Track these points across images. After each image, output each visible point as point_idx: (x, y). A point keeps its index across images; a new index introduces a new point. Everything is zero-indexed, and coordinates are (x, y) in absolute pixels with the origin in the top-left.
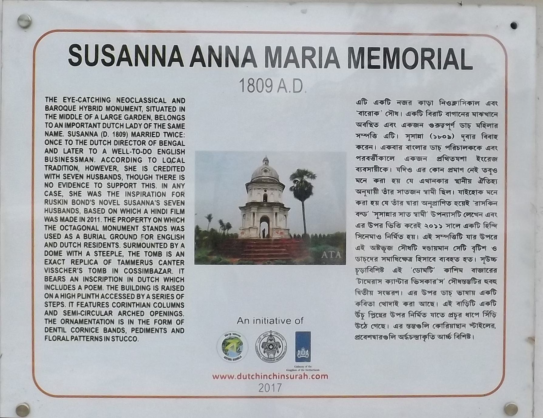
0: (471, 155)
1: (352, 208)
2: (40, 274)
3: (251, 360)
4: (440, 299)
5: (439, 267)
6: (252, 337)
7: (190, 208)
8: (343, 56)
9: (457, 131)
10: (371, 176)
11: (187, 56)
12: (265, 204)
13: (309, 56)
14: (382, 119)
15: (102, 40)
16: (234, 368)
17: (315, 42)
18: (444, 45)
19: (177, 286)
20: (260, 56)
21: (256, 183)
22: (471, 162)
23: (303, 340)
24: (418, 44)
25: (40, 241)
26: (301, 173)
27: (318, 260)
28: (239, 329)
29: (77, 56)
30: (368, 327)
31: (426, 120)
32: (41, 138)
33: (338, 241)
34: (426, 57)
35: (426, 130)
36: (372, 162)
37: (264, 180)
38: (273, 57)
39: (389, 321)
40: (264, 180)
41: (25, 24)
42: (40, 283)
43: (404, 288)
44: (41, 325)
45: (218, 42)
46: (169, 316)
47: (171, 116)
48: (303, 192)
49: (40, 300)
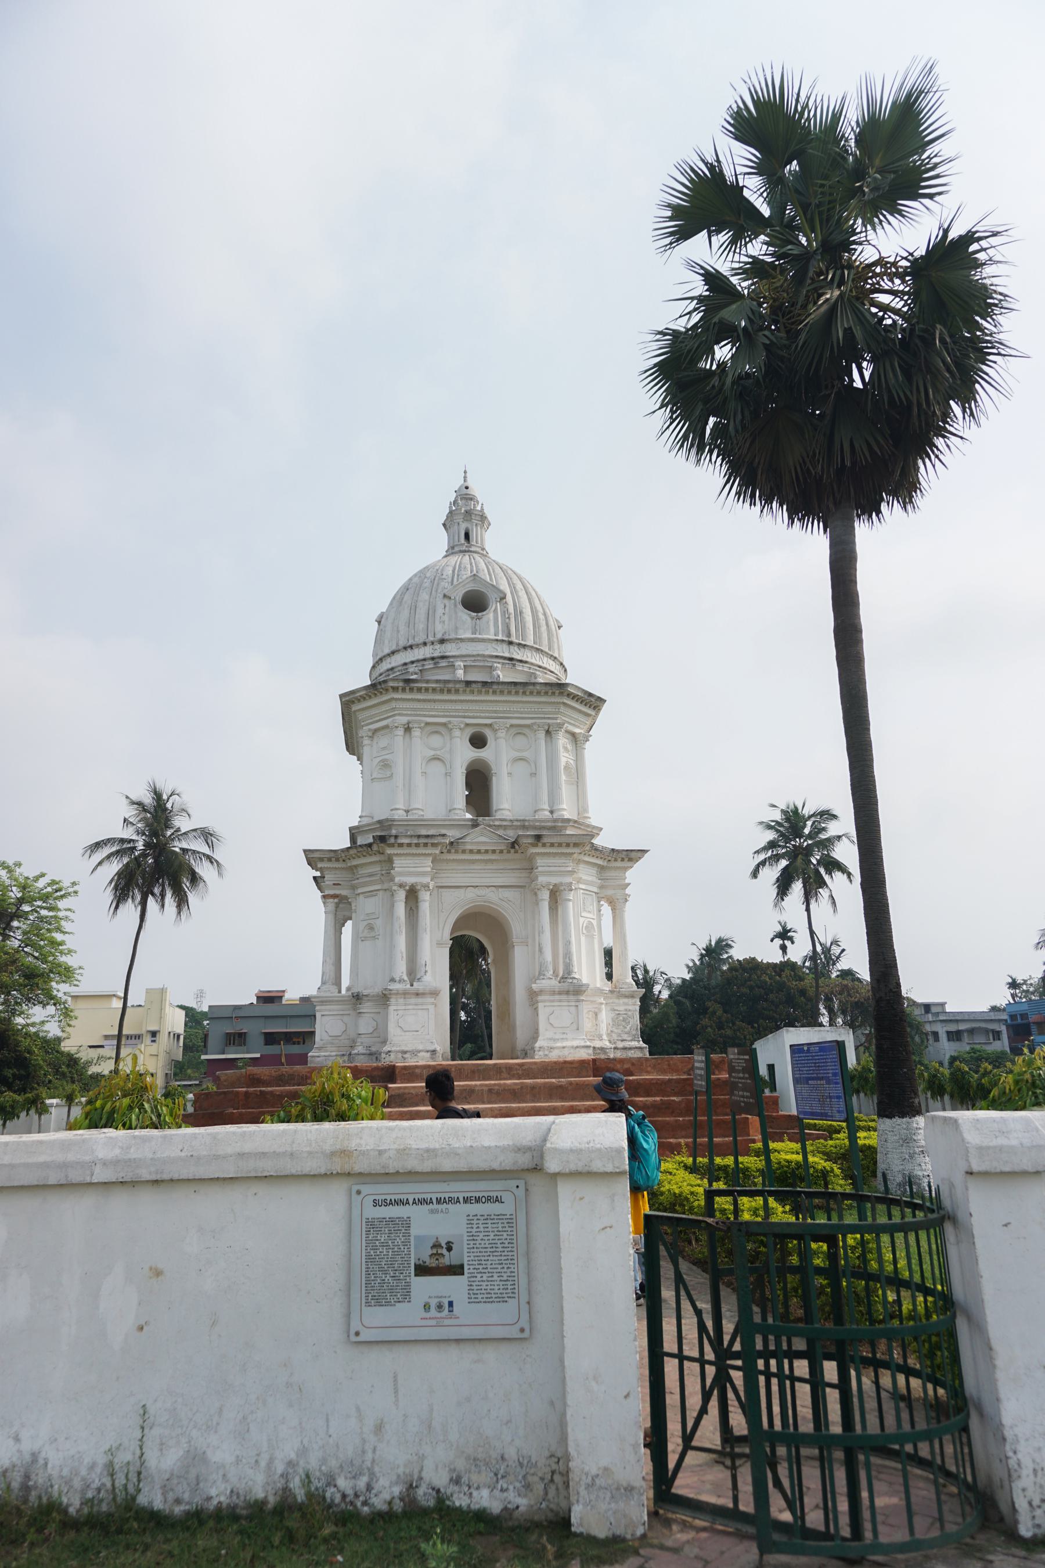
0: (505, 1234)
1: (466, 1254)
2: (364, 1282)
3: (433, 1312)
4: (496, 1287)
5: (495, 1278)
6: (433, 1303)
7: (412, 1256)
8: (461, 1200)
9: (500, 1225)
10: (472, 1242)
11: (411, 1202)
12: (437, 1254)
13: (451, 1200)
14: (475, 1222)
15: (384, 1197)
16: (428, 1315)
17: (452, 1195)
18: (495, 1194)
19: (408, 1285)
20: (434, 1201)
21: (434, 1246)
22: (505, 1236)
23: (451, 1304)
24: (486, 1194)
25: (364, 1270)
26: (448, 1243)
27: (455, 1274)
28: (430, 1300)
29: (376, 1203)
30: (473, 1299)
31: (489, 1221)
32: (364, 1233)
33: (462, 1266)
34: (489, 1199)
35: (490, 1225)
36: (472, 1237)
37: (437, 1245)
38: (439, 1201)
39: (480, 1296)
40: (437, 1245)
41: (359, 1192)
42: (364, 1286)
43: (484, 1284)
44: (364, 1301)
45: (421, 1196)
46: (406, 1296)
47: (406, 1223)
48: (449, 1249)
49: (364, 1292)
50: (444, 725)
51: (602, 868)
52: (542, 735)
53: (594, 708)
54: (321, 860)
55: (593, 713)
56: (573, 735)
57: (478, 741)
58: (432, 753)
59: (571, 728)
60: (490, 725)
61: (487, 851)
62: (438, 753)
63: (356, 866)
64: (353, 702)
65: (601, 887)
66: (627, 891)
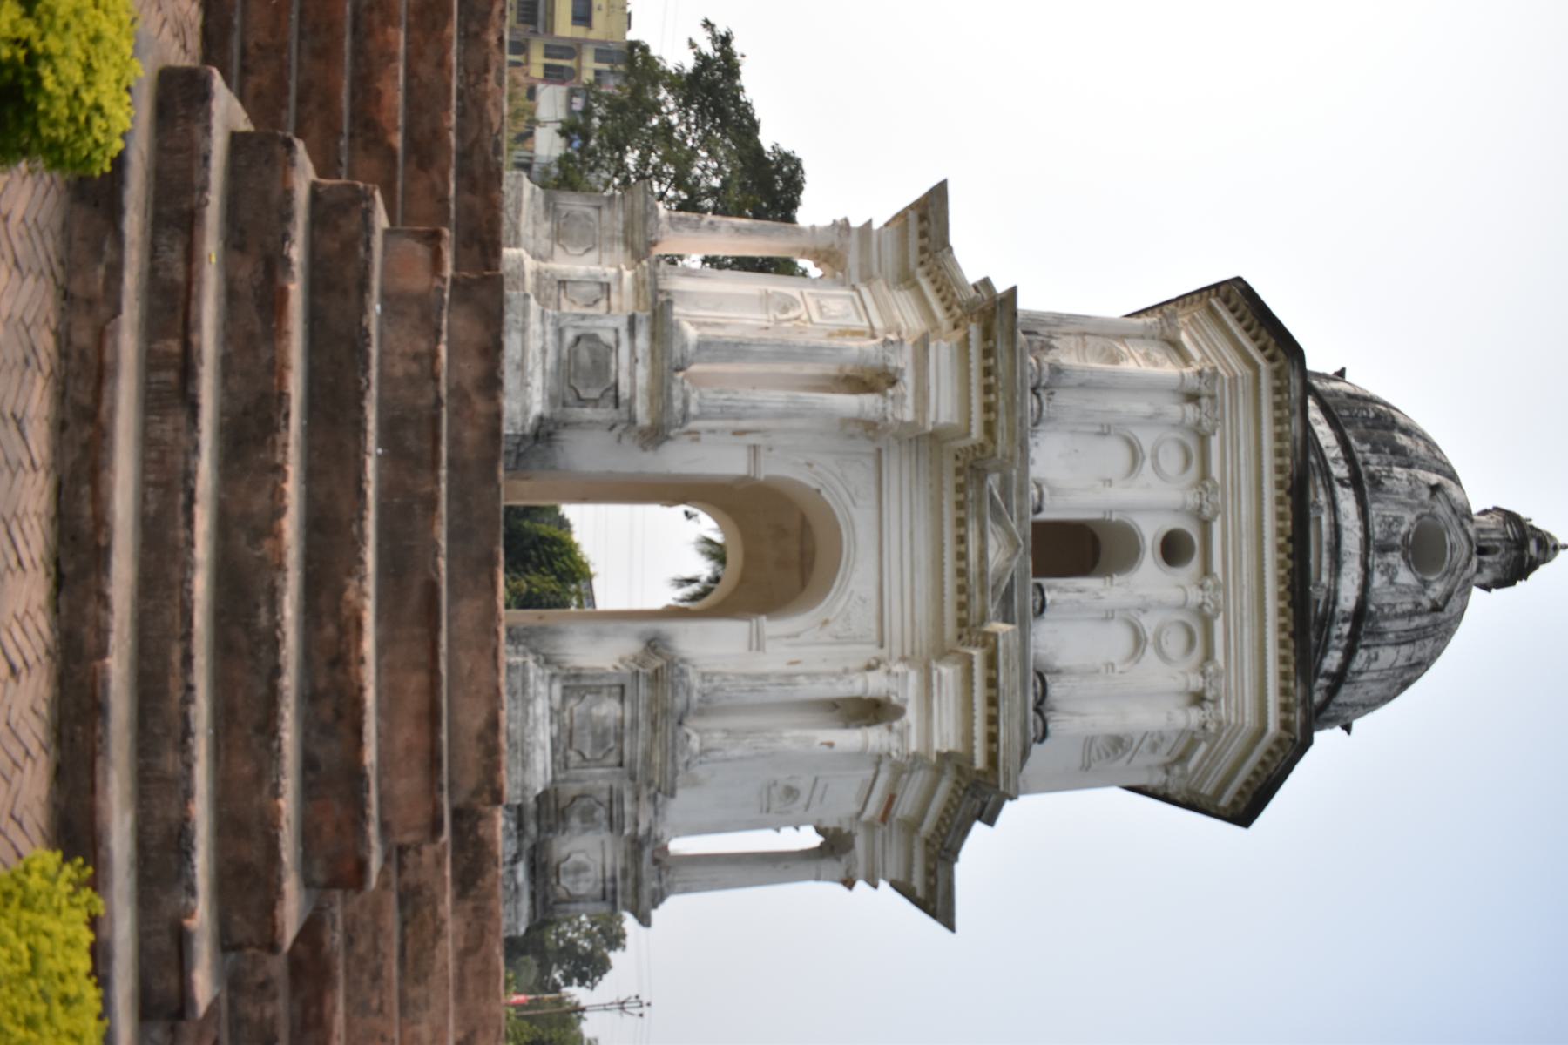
50: (1205, 474)
51: (912, 826)
52: (1196, 682)
53: (1234, 803)
54: (923, 218)
55: (1224, 802)
56: (1183, 758)
57: (1174, 549)
58: (1147, 448)
59: (1203, 747)
60: (1207, 571)
61: (962, 556)
62: (1148, 464)
63: (915, 285)
64: (1226, 301)
65: (870, 826)
66: (861, 885)
